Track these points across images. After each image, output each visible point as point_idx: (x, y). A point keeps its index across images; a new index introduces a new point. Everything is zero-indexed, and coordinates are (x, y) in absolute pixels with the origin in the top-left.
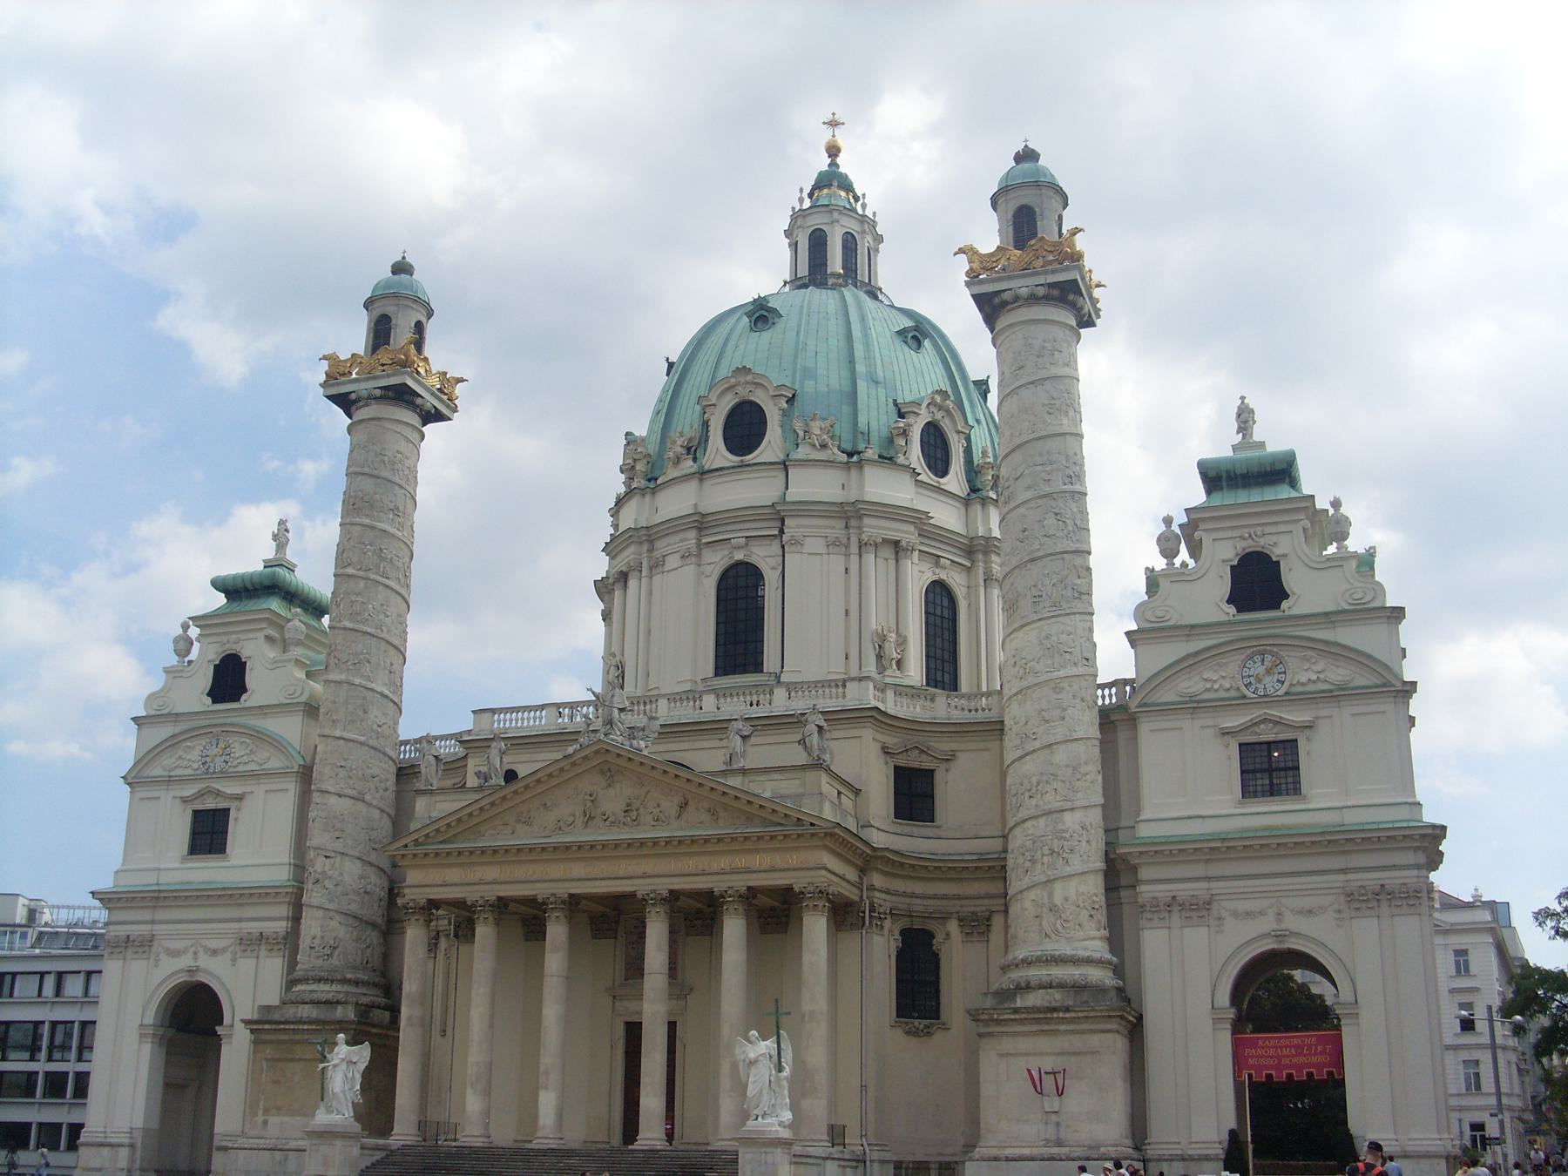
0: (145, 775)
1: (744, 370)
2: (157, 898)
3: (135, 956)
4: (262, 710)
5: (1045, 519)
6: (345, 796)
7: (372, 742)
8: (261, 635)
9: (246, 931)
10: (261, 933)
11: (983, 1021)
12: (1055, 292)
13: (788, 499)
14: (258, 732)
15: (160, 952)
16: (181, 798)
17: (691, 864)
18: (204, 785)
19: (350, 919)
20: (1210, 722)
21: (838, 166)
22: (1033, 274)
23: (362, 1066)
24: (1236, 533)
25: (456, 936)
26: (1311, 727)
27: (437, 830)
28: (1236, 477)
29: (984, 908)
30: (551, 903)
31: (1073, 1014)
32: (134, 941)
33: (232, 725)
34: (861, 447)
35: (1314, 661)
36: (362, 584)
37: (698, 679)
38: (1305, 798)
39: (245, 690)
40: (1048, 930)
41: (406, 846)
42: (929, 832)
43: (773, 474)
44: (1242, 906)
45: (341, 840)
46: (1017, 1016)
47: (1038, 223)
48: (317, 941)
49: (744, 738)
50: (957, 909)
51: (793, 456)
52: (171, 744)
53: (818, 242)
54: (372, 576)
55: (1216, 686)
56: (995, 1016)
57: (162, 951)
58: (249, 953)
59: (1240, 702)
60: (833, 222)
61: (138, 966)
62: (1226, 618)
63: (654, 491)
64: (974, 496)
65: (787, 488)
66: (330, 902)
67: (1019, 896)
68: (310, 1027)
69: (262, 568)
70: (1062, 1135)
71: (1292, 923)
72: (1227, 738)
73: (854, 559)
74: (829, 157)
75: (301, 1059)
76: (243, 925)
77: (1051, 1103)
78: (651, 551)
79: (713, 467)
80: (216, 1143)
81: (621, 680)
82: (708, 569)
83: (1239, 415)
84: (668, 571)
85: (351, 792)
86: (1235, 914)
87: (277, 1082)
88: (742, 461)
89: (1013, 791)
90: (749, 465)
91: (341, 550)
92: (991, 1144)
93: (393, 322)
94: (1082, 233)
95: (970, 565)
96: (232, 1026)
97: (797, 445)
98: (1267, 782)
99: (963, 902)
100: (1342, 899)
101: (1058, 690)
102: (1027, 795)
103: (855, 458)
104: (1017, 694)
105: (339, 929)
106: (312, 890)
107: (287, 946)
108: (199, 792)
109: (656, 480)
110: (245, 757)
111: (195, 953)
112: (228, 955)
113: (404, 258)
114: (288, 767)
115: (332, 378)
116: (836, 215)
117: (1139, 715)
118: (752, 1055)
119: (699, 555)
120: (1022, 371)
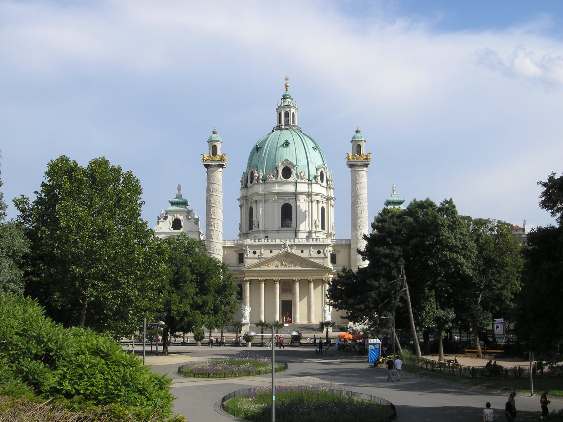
1: (287, 160)
12: (365, 165)
42: (335, 266)
49: (312, 251)
51: (298, 181)
53: (287, 114)
60: (290, 110)
64: (328, 187)
65: (296, 188)
73: (310, 204)
74: (286, 88)
82: (280, 204)
85: (217, 253)
95: (327, 202)
97: (298, 178)
103: (310, 181)
109: (265, 181)
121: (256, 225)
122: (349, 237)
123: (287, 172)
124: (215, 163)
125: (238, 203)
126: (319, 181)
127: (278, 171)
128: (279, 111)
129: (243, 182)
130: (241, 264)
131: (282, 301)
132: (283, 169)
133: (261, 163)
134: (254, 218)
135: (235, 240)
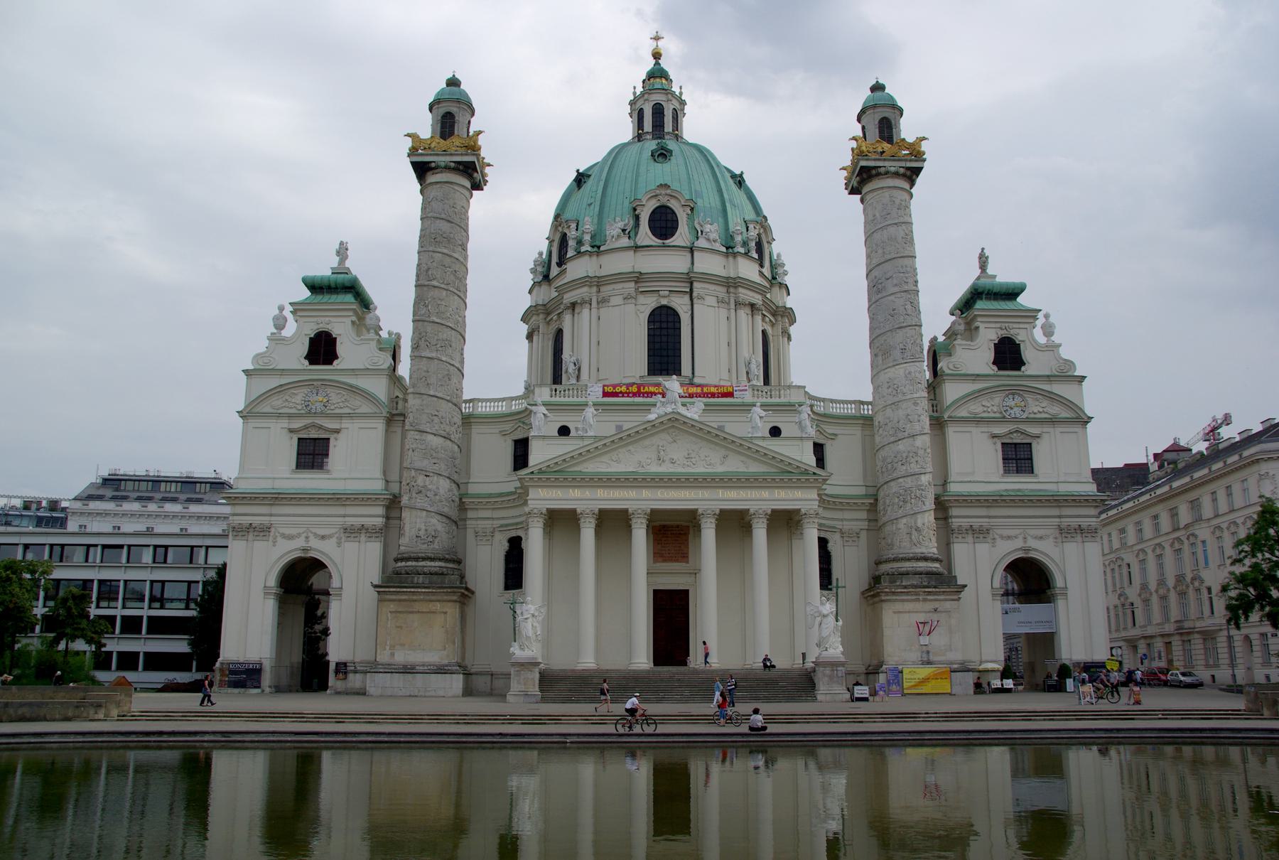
0: (256, 411)
1: (666, 186)
2: (277, 498)
3: (258, 538)
4: (353, 372)
5: (906, 305)
7: (454, 400)
8: (348, 321)
11: (886, 592)
12: (908, 173)
13: (695, 270)
14: (351, 386)
15: (277, 536)
16: (289, 429)
17: (732, 494)
18: (311, 421)
19: (444, 518)
20: (986, 430)
21: (660, 64)
22: (899, 160)
23: (540, 618)
24: (998, 325)
26: (1038, 437)
28: (991, 294)
29: (854, 527)
30: (639, 514)
31: (937, 590)
32: (256, 527)
34: (732, 244)
35: (1041, 401)
36: (444, 293)
37: (638, 376)
38: (1036, 475)
39: (336, 357)
40: (915, 541)
41: (532, 473)
43: (684, 254)
44: (1006, 532)
45: (437, 465)
46: (905, 590)
47: (894, 130)
49: (760, 417)
50: (841, 527)
51: (695, 245)
52: (280, 389)
53: (658, 111)
54: (451, 289)
55: (989, 410)
56: (893, 590)
57: (277, 534)
59: (1003, 420)
61: (260, 546)
62: (992, 372)
63: (599, 253)
64: (774, 282)
65: (693, 263)
66: (431, 506)
67: (895, 521)
68: (427, 590)
69: (330, 274)
70: (932, 658)
71: (1032, 543)
72: (996, 439)
75: (419, 612)
76: (347, 519)
77: (924, 640)
78: (599, 291)
79: (642, 245)
81: (577, 372)
82: (642, 308)
83: (980, 258)
86: (1002, 537)
87: (401, 627)
88: (664, 243)
89: (889, 460)
90: (669, 246)
91: (424, 267)
92: (890, 663)
93: (457, 118)
94: (926, 141)
95: (774, 321)
96: (342, 588)
97: (698, 238)
98: (1015, 465)
99: (845, 523)
100: (1057, 531)
101: (916, 404)
102: (900, 463)
103: (730, 250)
104: (890, 405)
105: (437, 524)
106: (416, 498)
107: (383, 535)
108: (305, 426)
109: (599, 247)
110: (341, 404)
111: (307, 538)
112: (334, 540)
113: (454, 76)
114: (376, 413)
115: (413, 151)
116: (670, 96)
117: (948, 422)
118: (825, 612)
119: (636, 299)
120: (888, 216)
121: (570, 370)
122: (865, 392)
123: (664, 223)
124: (448, 159)
125: (524, 328)
126: (756, 256)
127: (637, 218)
128: (638, 106)
129: (540, 269)
131: (654, 590)
132: (653, 212)
133: (590, 205)
134: (566, 355)
135: (503, 400)
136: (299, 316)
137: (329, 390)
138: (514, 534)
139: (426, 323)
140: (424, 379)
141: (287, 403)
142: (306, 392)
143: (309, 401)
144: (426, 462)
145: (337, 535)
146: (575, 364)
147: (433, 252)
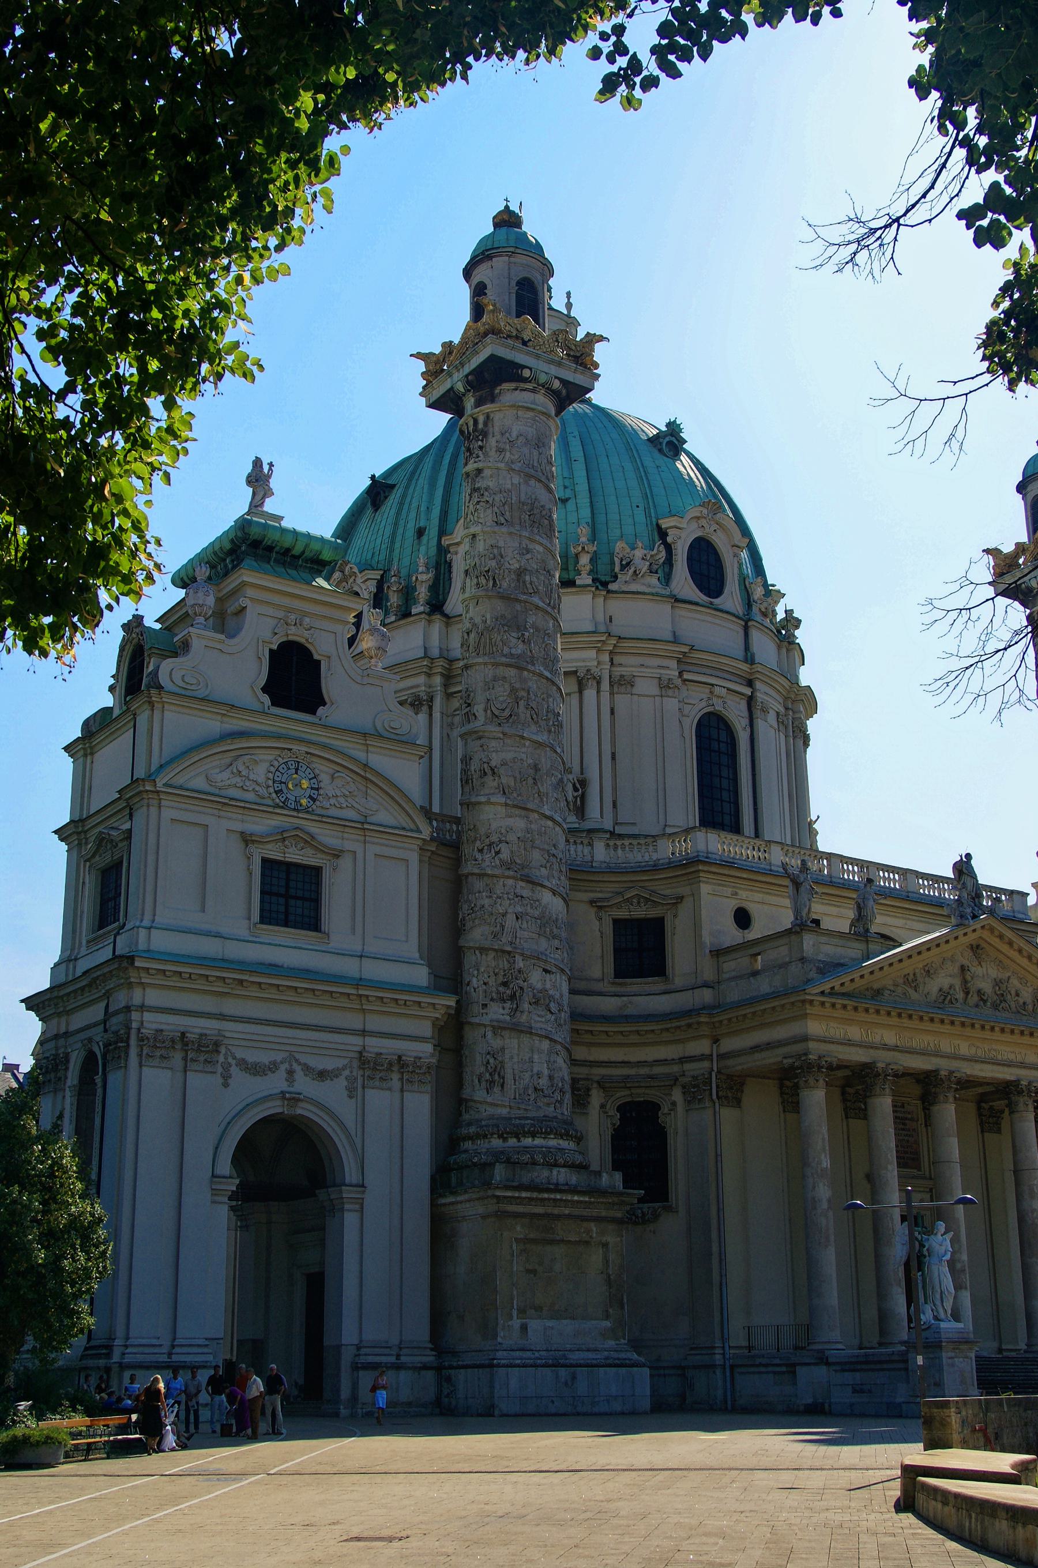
2: (241, 982)
6: (560, 895)
9: (376, 1050)
10: (400, 1057)
14: (366, 766)
25: (718, 1097)
27: (852, 980)
33: (325, 747)
41: (822, 993)
48: (543, 1082)
57: (230, 1060)
58: (377, 1083)
76: (370, 1041)
80: (347, 1357)
84: (639, 695)
87: (534, 1272)
88: (711, 603)
90: (721, 611)
96: (363, 1186)
109: (605, 584)
110: (342, 800)
111: (290, 1072)
112: (342, 1082)
114: (404, 829)
127: (668, 548)
130: (653, 984)
133: (567, 500)
136: (251, 599)
137: (319, 766)
138: (641, 1095)
139: (526, 673)
140: (530, 781)
141: (238, 779)
142: (276, 764)
143: (281, 782)
144: (543, 944)
145: (347, 1072)
146: (576, 789)
147: (530, 540)
